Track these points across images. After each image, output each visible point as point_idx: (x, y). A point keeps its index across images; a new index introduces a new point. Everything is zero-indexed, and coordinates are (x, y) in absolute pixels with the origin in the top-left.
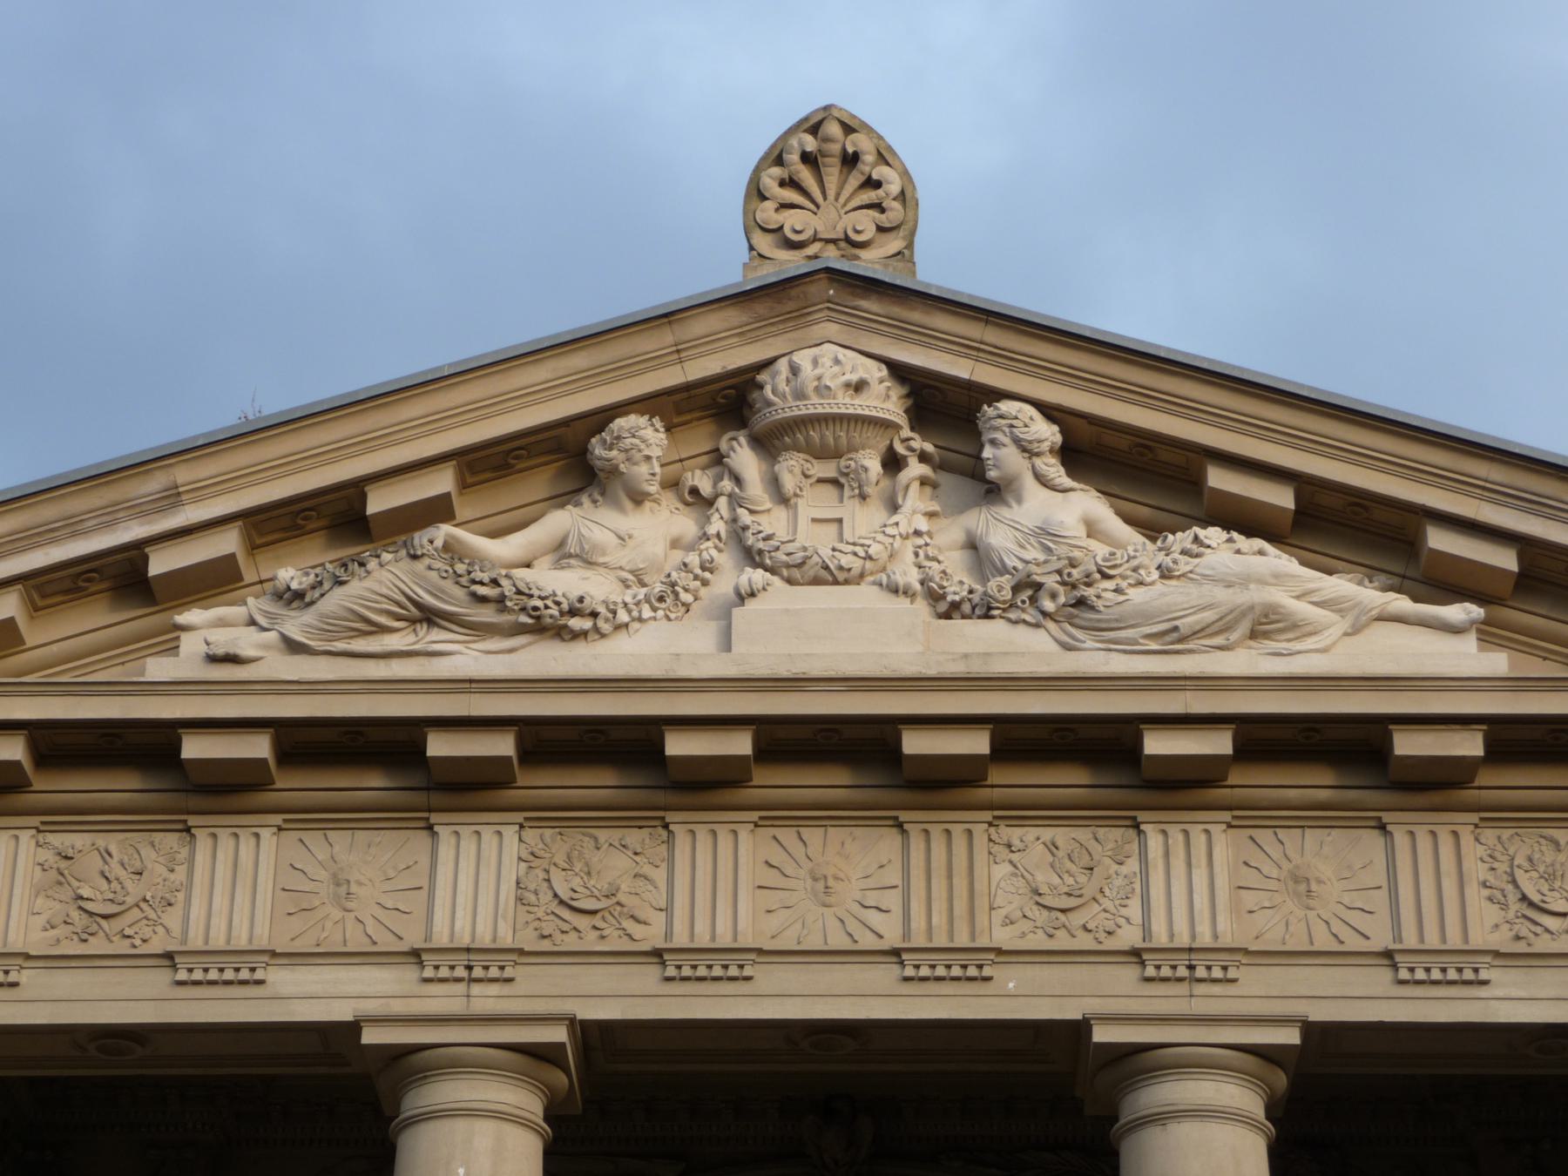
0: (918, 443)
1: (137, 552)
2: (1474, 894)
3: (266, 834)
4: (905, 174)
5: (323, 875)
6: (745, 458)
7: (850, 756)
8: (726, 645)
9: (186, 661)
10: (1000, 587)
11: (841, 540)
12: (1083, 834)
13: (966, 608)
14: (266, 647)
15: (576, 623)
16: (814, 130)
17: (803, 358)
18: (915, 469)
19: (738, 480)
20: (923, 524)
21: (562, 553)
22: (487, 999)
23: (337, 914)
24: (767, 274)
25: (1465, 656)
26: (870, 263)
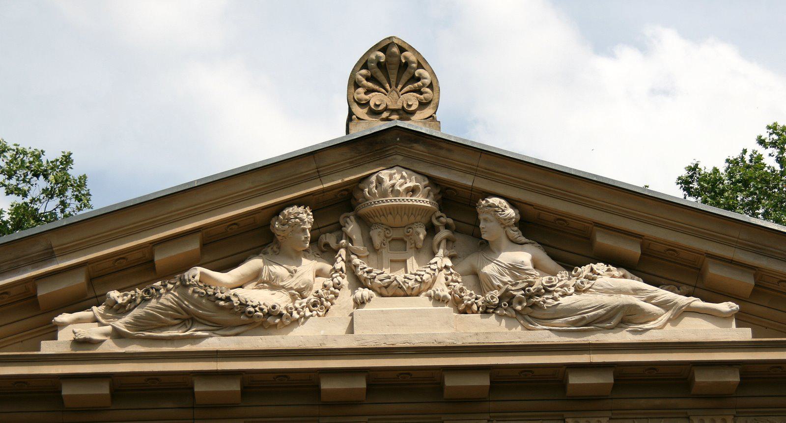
0: (443, 220)
4: (433, 73)
6: (352, 228)
9: (62, 343)
13: (475, 307)
14: (106, 335)
16: (384, 50)
18: (443, 233)
19: (350, 240)
20: (449, 263)
21: (256, 277)
24: (360, 130)
26: (415, 124)
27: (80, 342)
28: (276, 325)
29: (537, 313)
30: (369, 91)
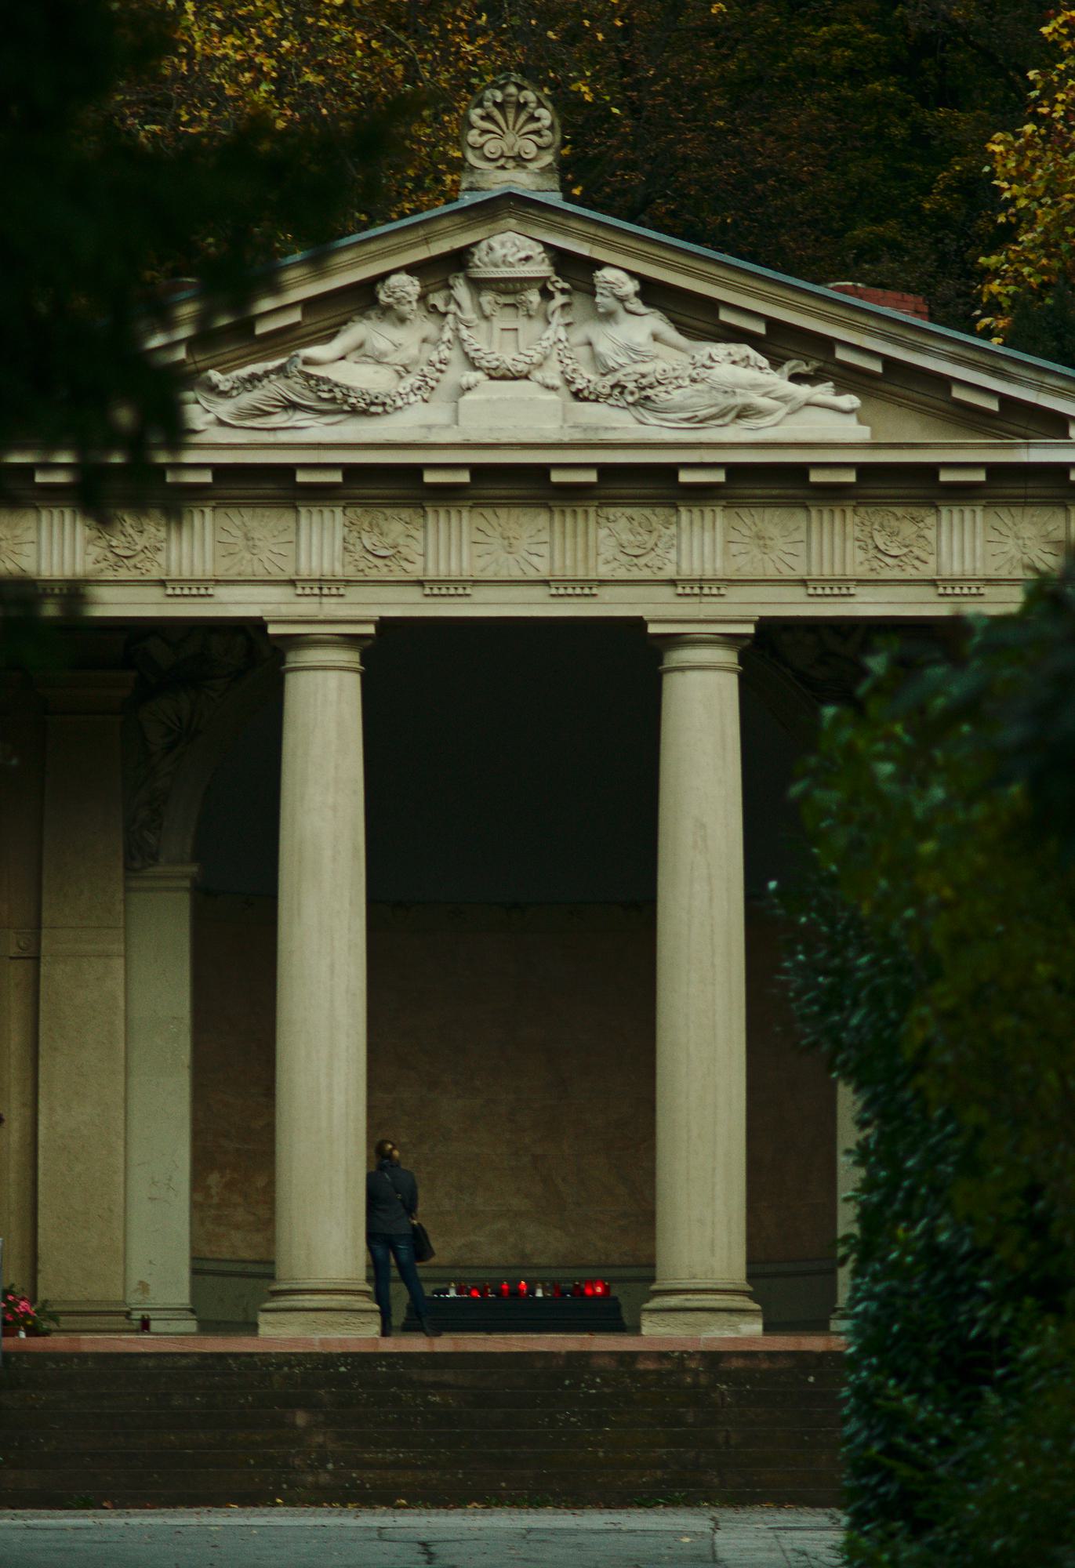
0: (561, 284)
3: (207, 511)
5: (238, 533)
6: (462, 292)
12: (647, 512)
15: (373, 409)
19: (459, 305)
22: (331, 608)
23: (248, 556)
28: (377, 414)
29: (650, 404)
30: (484, 132)
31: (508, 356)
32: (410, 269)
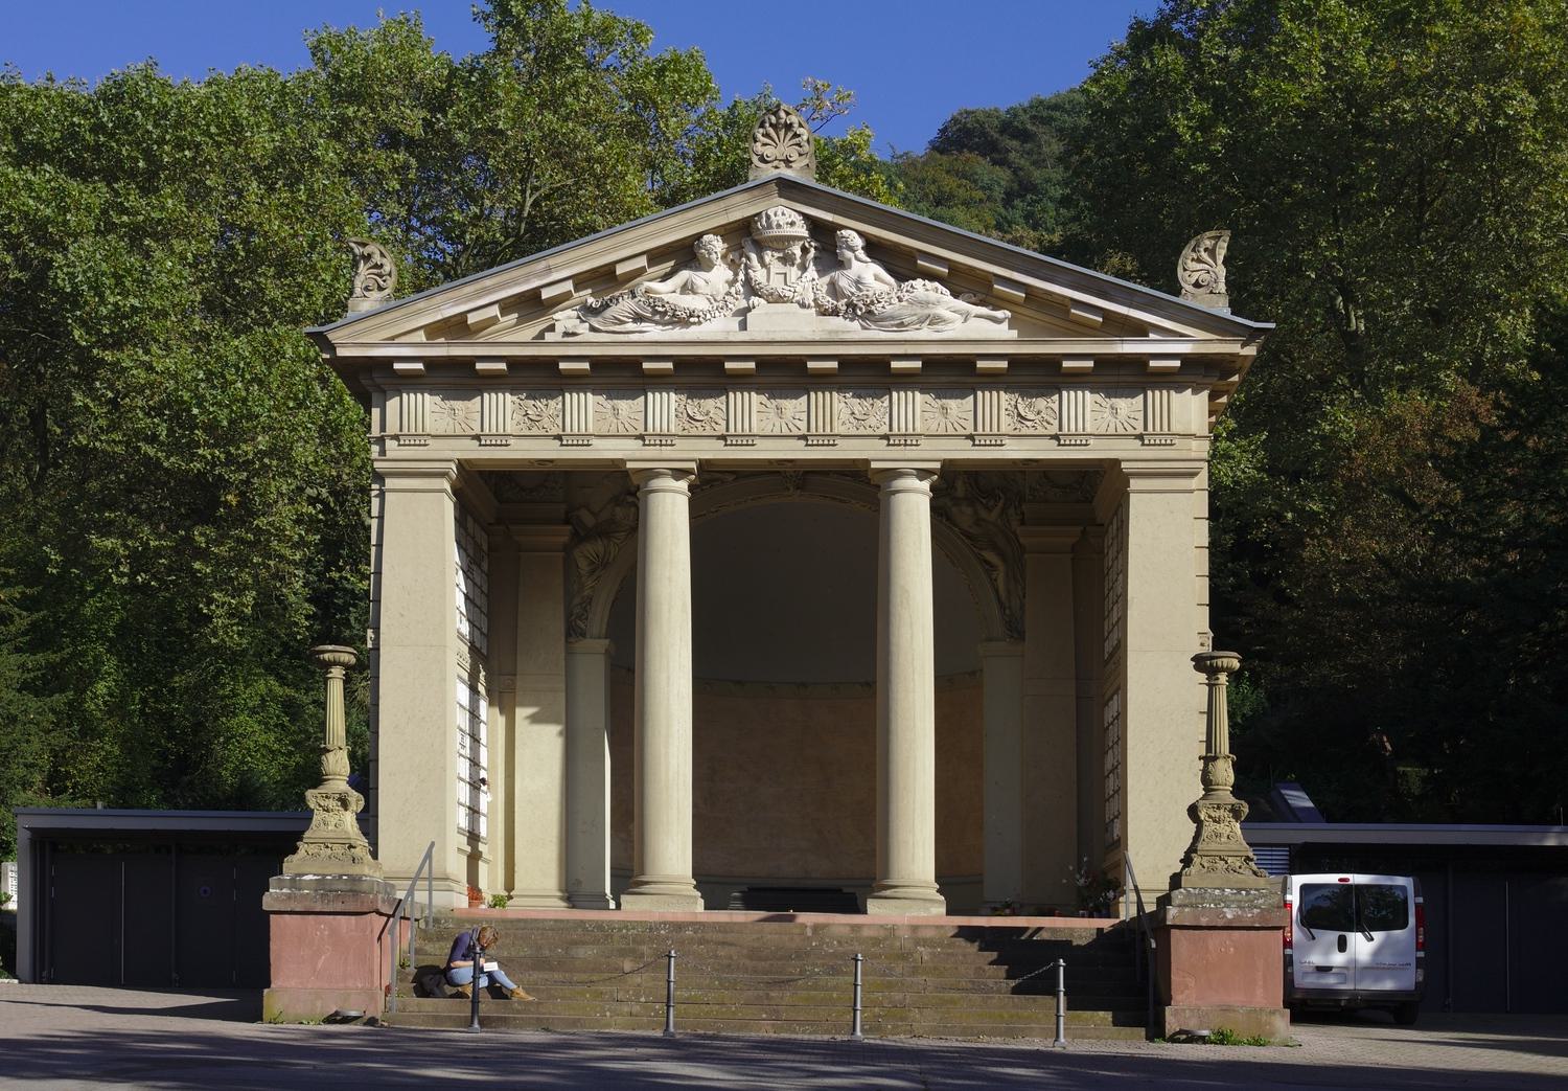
1: (536, 292)
2: (1003, 412)
7: (783, 374)
8: (743, 326)
10: (842, 304)
11: (786, 284)
15: (692, 320)
17: (771, 212)
22: (667, 452)
25: (1004, 331)
27: (566, 334)
28: (694, 323)
29: (872, 318)
30: (765, 145)
31: (776, 283)
32: (715, 231)
